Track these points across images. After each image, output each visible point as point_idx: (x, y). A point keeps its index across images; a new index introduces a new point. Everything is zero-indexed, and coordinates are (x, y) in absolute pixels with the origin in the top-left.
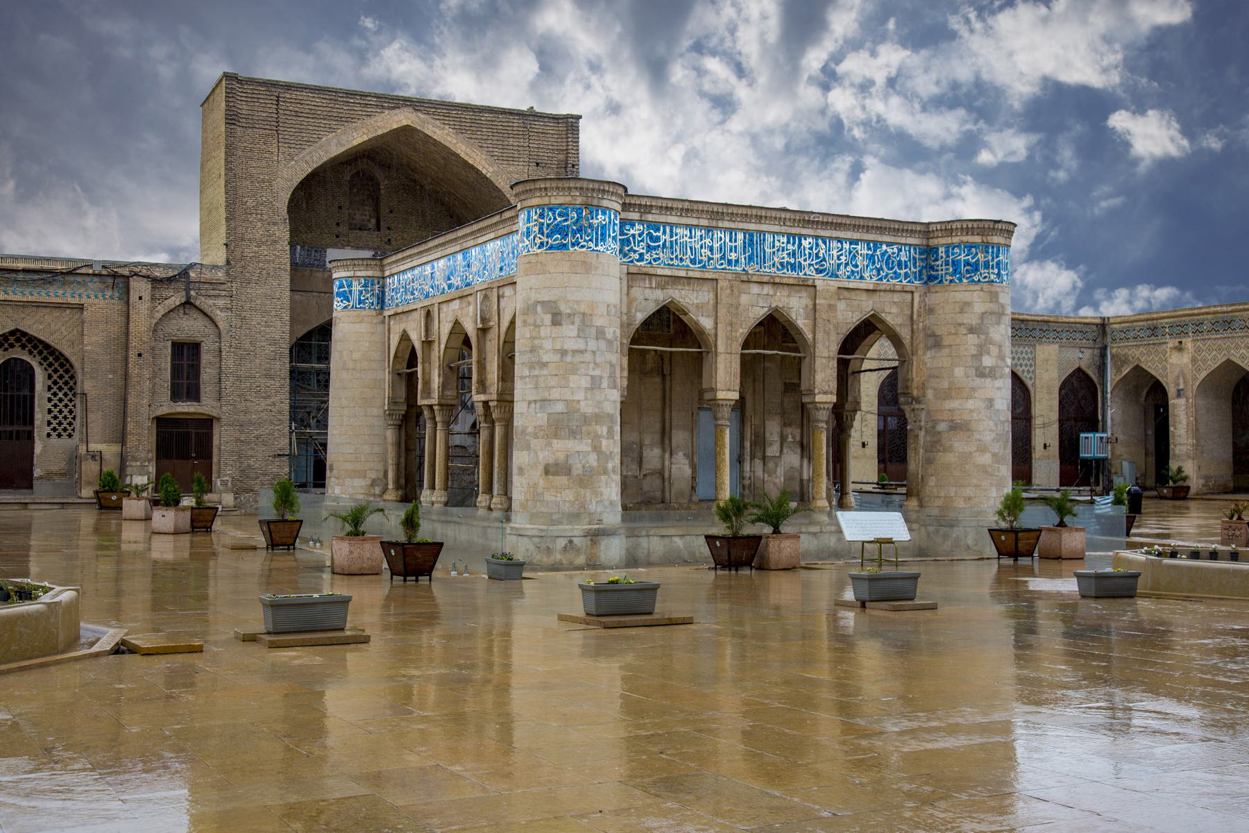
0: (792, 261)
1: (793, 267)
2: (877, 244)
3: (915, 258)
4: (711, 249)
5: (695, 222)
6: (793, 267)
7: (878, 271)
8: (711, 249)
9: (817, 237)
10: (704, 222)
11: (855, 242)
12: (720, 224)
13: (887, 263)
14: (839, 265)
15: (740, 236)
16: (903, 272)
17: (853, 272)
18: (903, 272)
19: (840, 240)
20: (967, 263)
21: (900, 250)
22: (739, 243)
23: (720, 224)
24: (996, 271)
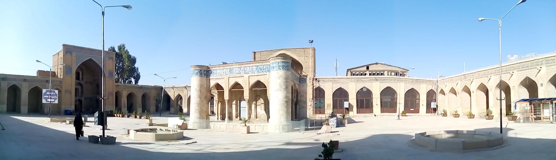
0: (239, 72)
1: (239, 73)
2: (258, 66)
3: (267, 68)
4: (224, 73)
5: (220, 68)
6: (239, 73)
7: (258, 71)
8: (224, 73)
9: (244, 67)
10: (222, 68)
11: (253, 66)
12: (225, 68)
13: (260, 69)
14: (249, 72)
15: (229, 69)
16: (264, 70)
17: (252, 72)
18: (264, 70)
19: (249, 67)
20: (273, 67)
21: (263, 66)
22: (229, 71)
23: (225, 68)
24: (278, 68)
